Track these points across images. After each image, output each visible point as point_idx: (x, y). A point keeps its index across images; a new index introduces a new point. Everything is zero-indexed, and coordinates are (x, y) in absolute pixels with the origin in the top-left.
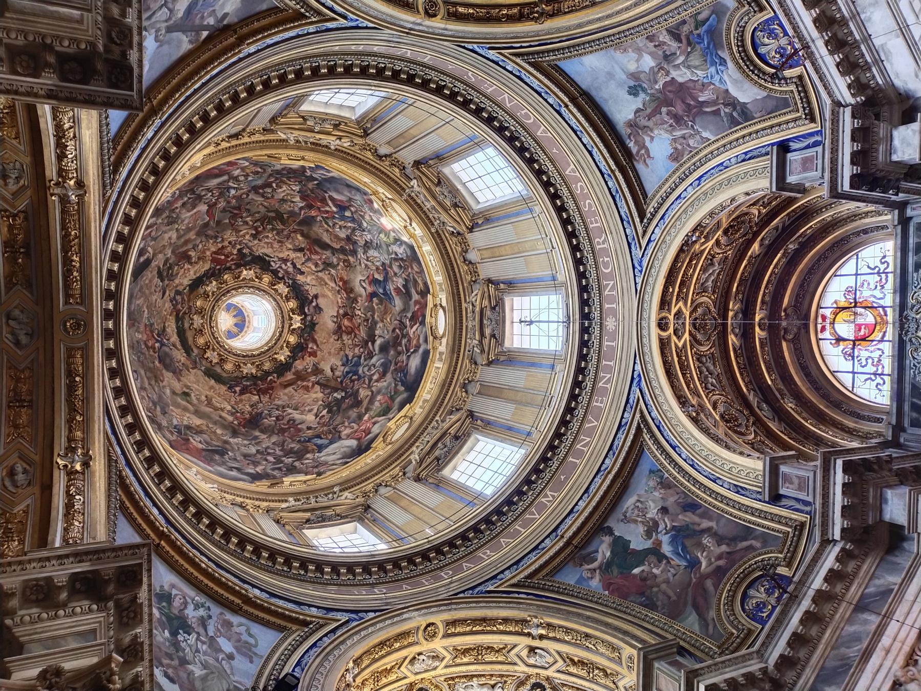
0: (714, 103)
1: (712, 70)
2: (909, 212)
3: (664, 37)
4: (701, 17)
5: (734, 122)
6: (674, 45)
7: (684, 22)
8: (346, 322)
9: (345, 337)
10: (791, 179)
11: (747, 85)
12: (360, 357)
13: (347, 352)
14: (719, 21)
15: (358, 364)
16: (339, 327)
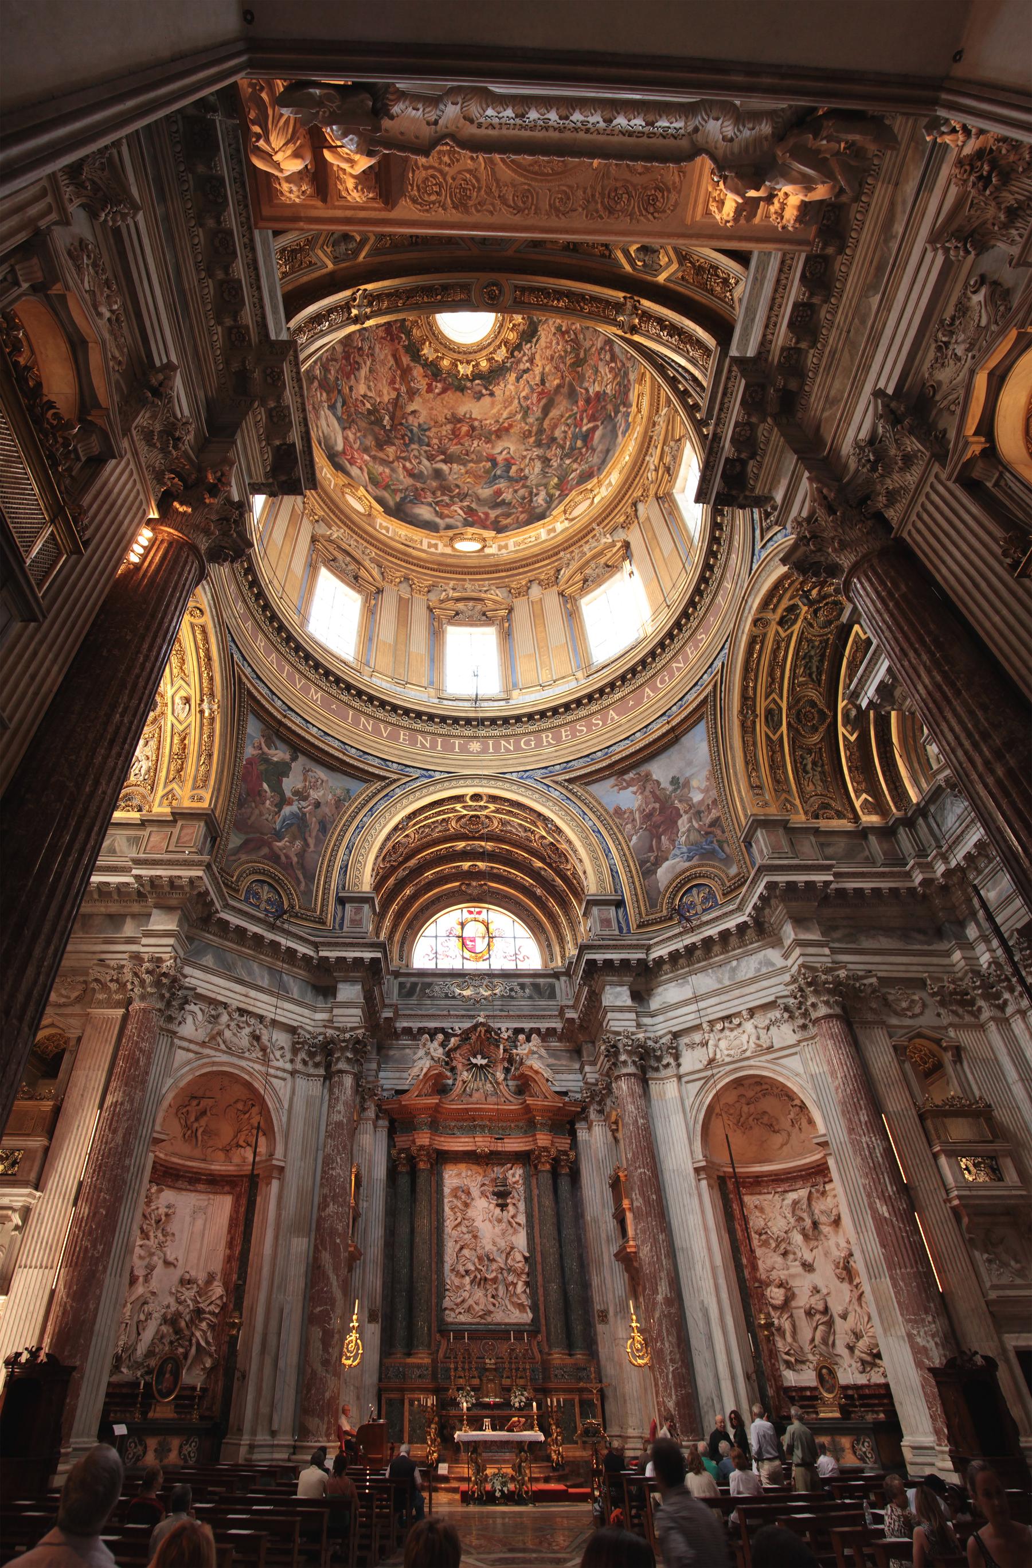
0: (659, 848)
1: (685, 849)
2: (563, 979)
3: (714, 813)
4: (725, 846)
5: (642, 863)
6: (708, 821)
7: (723, 832)
8: (465, 429)
9: (449, 427)
10: (595, 910)
11: (670, 876)
12: (428, 445)
13: (433, 430)
14: (721, 860)
15: (420, 442)
16: (460, 421)
